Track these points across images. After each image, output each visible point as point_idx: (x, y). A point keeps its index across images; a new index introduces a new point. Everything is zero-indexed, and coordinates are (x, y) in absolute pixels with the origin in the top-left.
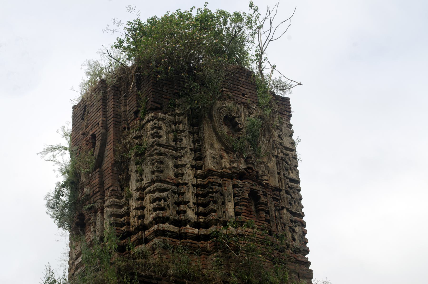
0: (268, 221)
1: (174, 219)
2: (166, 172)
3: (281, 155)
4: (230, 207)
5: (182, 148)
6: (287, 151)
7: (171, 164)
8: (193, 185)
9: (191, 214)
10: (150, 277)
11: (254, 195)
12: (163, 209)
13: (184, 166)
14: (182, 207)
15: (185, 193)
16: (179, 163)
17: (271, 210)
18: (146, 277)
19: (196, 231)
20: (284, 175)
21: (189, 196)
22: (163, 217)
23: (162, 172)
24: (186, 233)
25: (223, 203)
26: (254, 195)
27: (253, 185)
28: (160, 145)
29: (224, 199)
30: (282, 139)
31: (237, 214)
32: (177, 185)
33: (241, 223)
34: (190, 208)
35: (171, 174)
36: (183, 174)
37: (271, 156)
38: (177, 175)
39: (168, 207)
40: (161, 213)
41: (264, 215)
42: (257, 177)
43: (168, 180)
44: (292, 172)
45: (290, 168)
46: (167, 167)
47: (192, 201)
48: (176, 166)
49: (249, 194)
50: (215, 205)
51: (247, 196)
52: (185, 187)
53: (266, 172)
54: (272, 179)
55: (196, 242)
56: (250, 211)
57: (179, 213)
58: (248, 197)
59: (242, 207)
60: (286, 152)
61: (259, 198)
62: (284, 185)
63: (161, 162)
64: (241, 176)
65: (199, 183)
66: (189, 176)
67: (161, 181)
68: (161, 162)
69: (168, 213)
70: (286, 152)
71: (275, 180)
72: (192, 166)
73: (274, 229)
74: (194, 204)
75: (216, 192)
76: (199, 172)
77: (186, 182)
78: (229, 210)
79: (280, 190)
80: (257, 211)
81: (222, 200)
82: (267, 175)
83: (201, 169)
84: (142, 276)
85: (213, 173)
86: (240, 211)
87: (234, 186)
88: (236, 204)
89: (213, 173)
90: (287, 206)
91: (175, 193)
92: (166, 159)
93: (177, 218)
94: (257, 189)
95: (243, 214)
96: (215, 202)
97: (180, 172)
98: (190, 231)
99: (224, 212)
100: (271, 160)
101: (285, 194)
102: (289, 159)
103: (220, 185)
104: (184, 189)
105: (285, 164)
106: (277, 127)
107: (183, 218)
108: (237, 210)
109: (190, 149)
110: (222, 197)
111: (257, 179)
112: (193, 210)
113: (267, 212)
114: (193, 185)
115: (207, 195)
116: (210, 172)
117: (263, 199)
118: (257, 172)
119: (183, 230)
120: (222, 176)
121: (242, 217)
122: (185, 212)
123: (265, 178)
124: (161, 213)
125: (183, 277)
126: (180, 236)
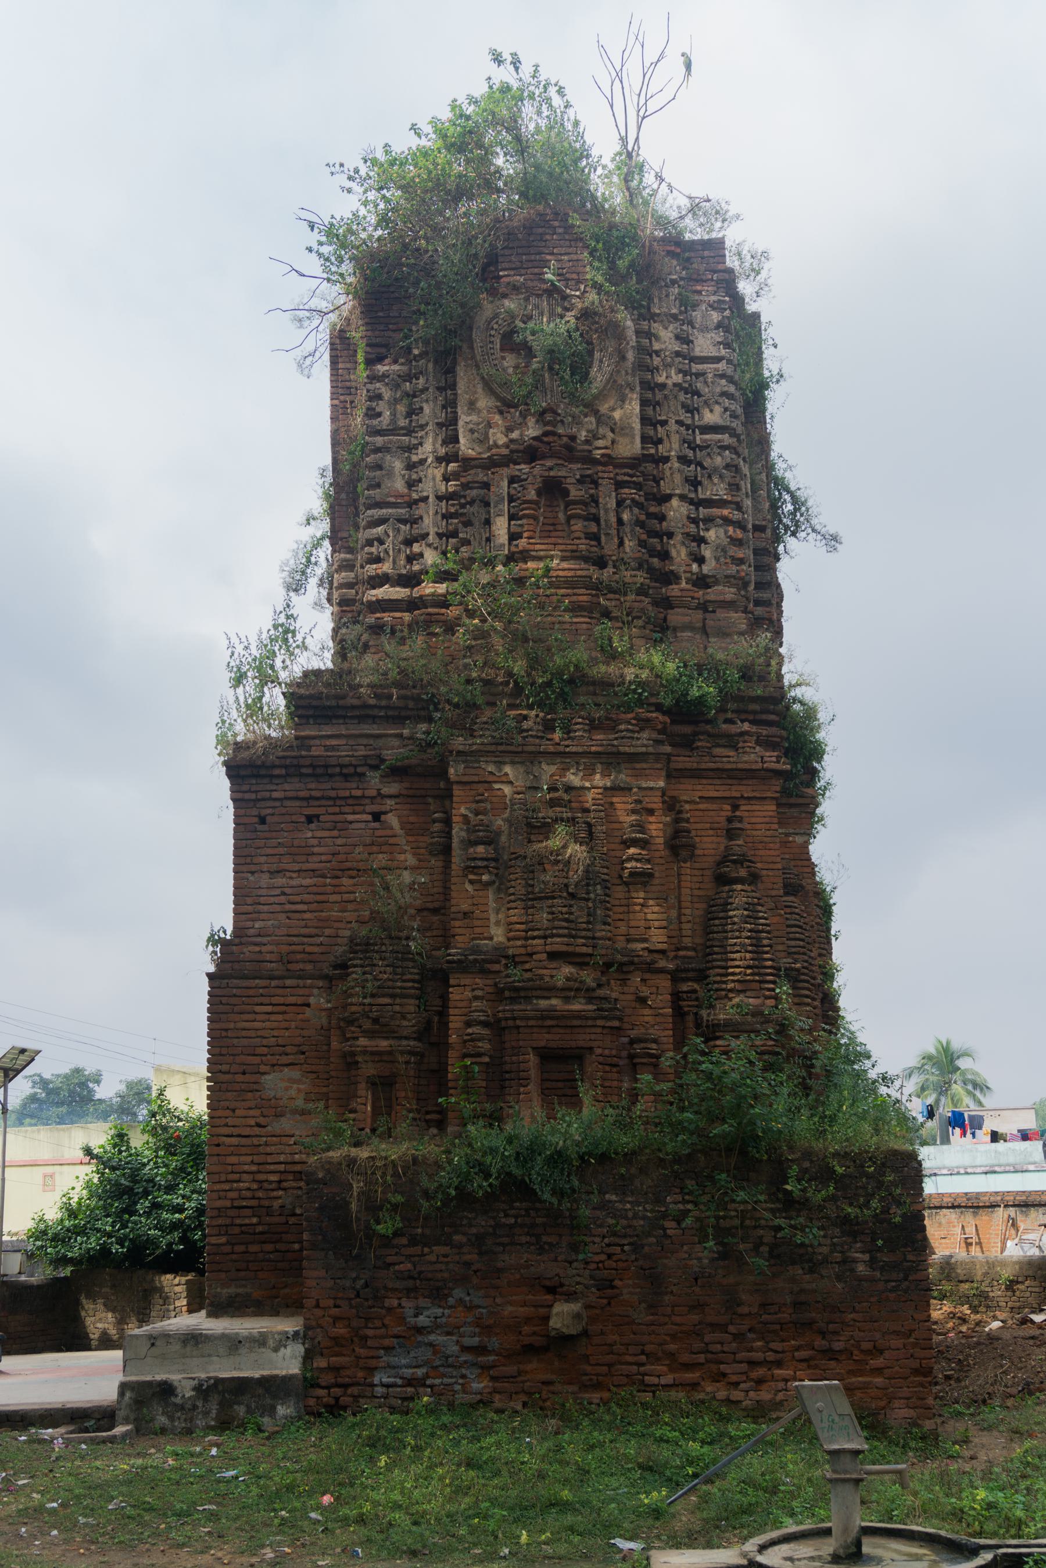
0: (595, 537)
1: (400, 576)
2: (387, 483)
3: (678, 378)
4: (501, 527)
5: (422, 427)
6: (700, 367)
7: (398, 465)
8: (439, 498)
9: (431, 557)
10: (319, 696)
11: (553, 489)
12: (378, 560)
13: (422, 462)
14: (416, 548)
15: (421, 518)
16: (415, 458)
17: (606, 511)
18: (311, 697)
19: (442, 588)
20: (677, 422)
21: (430, 522)
22: (377, 575)
23: (378, 485)
24: (421, 597)
25: (488, 522)
26: (553, 489)
27: (551, 469)
28: (379, 433)
29: (489, 512)
30: (688, 341)
31: (513, 537)
32: (412, 504)
33: (525, 556)
34: (429, 545)
35: (399, 485)
36: (420, 481)
37: (627, 391)
38: (411, 484)
39: (386, 552)
40: (371, 569)
41: (578, 526)
42: (569, 449)
43: (392, 500)
44: (711, 411)
45: (706, 402)
46: (390, 474)
47: (432, 531)
48: (410, 466)
49: (539, 493)
50: (469, 529)
51: (532, 495)
52: (422, 505)
53: (603, 430)
54: (622, 441)
55: (443, 611)
56: (554, 524)
57: (410, 559)
58: (535, 498)
59: (524, 521)
60: (696, 368)
61: (566, 493)
62: (676, 446)
63: (379, 467)
64: (531, 454)
65: (450, 490)
66: (434, 480)
67: (379, 505)
68: (379, 467)
69: (386, 567)
70: (696, 368)
71: (632, 443)
72: (439, 460)
73: (609, 547)
74: (440, 535)
75: (472, 503)
76: (452, 466)
77: (425, 494)
78: (497, 533)
79: (666, 459)
80: (569, 519)
81: (484, 516)
82: (604, 437)
83: (457, 461)
84: (301, 697)
85: (473, 463)
86: (519, 530)
87: (512, 480)
88: (512, 517)
89: (473, 463)
90: (677, 492)
91: (404, 522)
92: (388, 457)
93: (404, 572)
94: (560, 474)
95: (525, 535)
96: (468, 524)
97: (414, 476)
98: (428, 591)
99: (488, 540)
100: (623, 401)
101: (676, 465)
102: (706, 382)
103: (486, 486)
104: (420, 510)
105: (682, 397)
106: (675, 317)
107: (416, 567)
108: (513, 529)
109: (438, 424)
110: (482, 510)
111: (570, 452)
112: (436, 548)
113: (596, 519)
114: (439, 498)
115: (464, 511)
116: (467, 463)
117: (575, 493)
118: (573, 438)
119: (416, 592)
120: (493, 464)
121: (522, 543)
122: (421, 555)
123: (600, 443)
124: (371, 569)
125: (397, 684)
126: (411, 605)
